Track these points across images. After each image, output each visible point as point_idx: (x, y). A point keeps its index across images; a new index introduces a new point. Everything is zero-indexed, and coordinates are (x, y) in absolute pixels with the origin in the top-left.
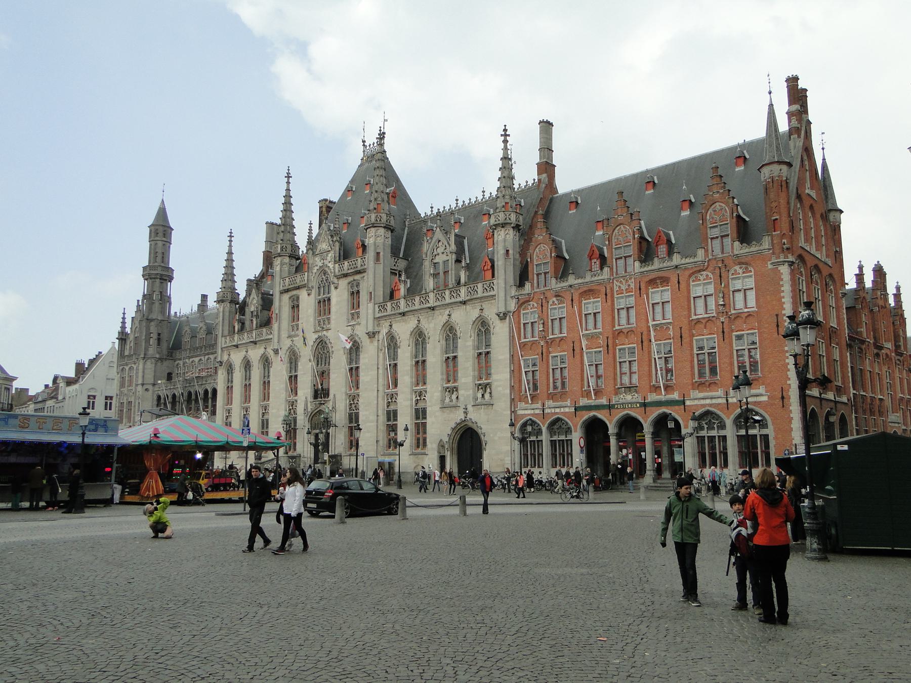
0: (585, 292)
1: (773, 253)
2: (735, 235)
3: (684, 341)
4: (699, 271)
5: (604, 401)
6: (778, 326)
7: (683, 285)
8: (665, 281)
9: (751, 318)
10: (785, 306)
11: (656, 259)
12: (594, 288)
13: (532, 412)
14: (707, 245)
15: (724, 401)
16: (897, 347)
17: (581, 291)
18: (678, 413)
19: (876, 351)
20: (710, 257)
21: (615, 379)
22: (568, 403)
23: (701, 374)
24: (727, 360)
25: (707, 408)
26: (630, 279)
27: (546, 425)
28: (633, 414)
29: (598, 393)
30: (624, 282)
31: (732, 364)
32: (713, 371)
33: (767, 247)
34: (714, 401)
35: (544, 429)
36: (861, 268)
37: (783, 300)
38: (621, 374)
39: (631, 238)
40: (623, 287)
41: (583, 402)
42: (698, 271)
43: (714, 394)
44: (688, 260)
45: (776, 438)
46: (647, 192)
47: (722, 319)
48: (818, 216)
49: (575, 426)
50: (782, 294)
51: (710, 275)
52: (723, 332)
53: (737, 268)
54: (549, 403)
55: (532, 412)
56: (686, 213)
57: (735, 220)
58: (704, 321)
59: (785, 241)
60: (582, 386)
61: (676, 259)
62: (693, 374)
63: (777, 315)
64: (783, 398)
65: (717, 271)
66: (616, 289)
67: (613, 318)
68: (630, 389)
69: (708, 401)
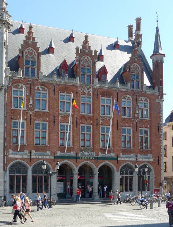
3: (119, 128)
4: (127, 94)
5: (73, 154)
15: (135, 159)
18: (113, 164)
22: (48, 152)
27: (32, 166)
29: (69, 150)
30: (86, 89)
34: (131, 159)
38: (90, 140)
40: (86, 92)
41: (59, 154)
43: (130, 156)
51: (131, 98)
54: (34, 152)
55: (21, 157)
64: (159, 160)
68: (86, 149)
69: (128, 159)
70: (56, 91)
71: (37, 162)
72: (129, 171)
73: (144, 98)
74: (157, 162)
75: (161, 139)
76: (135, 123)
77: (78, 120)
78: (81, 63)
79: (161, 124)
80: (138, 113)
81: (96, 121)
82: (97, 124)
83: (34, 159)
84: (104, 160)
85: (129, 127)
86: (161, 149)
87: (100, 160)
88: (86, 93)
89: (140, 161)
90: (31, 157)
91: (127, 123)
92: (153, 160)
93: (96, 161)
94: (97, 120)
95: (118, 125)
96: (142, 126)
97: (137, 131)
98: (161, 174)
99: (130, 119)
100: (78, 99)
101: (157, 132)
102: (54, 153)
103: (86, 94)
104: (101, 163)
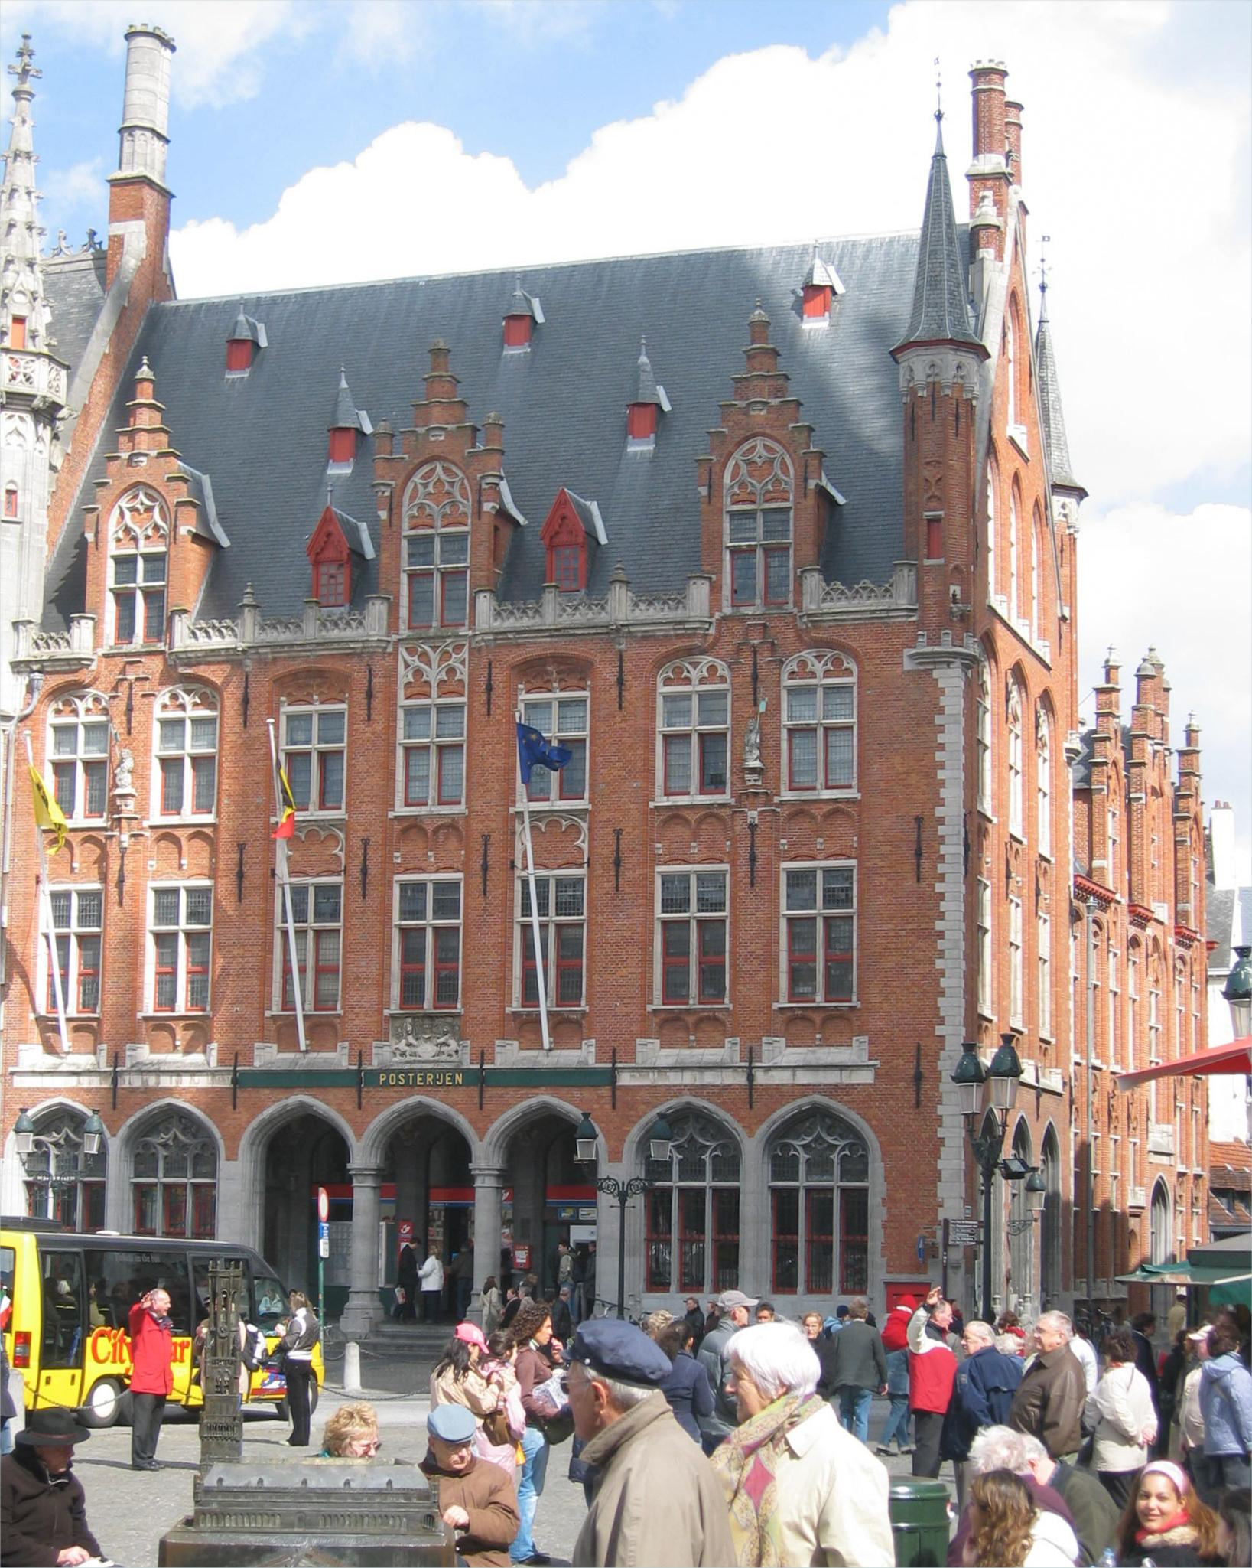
0: (295, 675)
1: (920, 625)
2: (809, 551)
3: (628, 875)
4: (690, 652)
5: (338, 1058)
6: (919, 854)
7: (634, 690)
8: (574, 670)
9: (839, 820)
10: (943, 793)
11: (550, 599)
12: (329, 665)
13: (72, 1082)
14: (719, 572)
15: (741, 1079)
16: (1180, 916)
17: (280, 670)
19: (1133, 930)
20: (727, 610)
21: (383, 986)
23: (674, 988)
24: (757, 948)
25: (687, 1098)
26: (458, 648)
27: (123, 1131)
28: (436, 1103)
30: (434, 657)
31: (772, 961)
32: (712, 977)
33: (903, 603)
34: (709, 1078)
35: (115, 1145)
36: (1110, 670)
37: (941, 774)
39: (466, 506)
40: (434, 674)
41: (267, 1056)
42: (681, 648)
44: (654, 613)
45: (889, 1201)
46: (510, 351)
47: (753, 815)
48: (1029, 505)
49: (233, 1141)
50: (939, 756)
51: (722, 668)
52: (753, 859)
53: (808, 655)
56: (641, 448)
57: (811, 501)
58: (693, 817)
59: (955, 589)
60: (264, 1003)
61: (621, 606)
62: (647, 988)
63: (919, 820)
64: (918, 1078)
65: (746, 660)
66: (404, 676)
67: (391, 776)
69: (687, 1078)
70: (253, 703)
71: (147, 1109)
72: (706, 1157)
73: (819, 658)
74: (904, 1089)
75: (939, 925)
76: (741, 829)
77: (370, 852)
78: (407, 511)
79: (941, 821)
80: (757, 764)
81: (477, 845)
82: (485, 868)
83: (133, 1090)
84: (524, 1091)
85: (711, 860)
86: (942, 994)
87: (500, 1091)
88: (434, 684)
89: (778, 1087)
90: (115, 1082)
91: (695, 837)
92: (877, 1076)
93: (476, 1094)
94: (486, 839)
95: (617, 863)
96: (805, 851)
97: (752, 884)
98: (939, 1172)
99: (709, 813)
100: (379, 727)
101: (910, 883)
102: (234, 1055)
103: (434, 692)
104: (509, 1106)
